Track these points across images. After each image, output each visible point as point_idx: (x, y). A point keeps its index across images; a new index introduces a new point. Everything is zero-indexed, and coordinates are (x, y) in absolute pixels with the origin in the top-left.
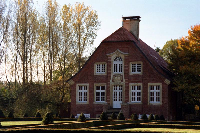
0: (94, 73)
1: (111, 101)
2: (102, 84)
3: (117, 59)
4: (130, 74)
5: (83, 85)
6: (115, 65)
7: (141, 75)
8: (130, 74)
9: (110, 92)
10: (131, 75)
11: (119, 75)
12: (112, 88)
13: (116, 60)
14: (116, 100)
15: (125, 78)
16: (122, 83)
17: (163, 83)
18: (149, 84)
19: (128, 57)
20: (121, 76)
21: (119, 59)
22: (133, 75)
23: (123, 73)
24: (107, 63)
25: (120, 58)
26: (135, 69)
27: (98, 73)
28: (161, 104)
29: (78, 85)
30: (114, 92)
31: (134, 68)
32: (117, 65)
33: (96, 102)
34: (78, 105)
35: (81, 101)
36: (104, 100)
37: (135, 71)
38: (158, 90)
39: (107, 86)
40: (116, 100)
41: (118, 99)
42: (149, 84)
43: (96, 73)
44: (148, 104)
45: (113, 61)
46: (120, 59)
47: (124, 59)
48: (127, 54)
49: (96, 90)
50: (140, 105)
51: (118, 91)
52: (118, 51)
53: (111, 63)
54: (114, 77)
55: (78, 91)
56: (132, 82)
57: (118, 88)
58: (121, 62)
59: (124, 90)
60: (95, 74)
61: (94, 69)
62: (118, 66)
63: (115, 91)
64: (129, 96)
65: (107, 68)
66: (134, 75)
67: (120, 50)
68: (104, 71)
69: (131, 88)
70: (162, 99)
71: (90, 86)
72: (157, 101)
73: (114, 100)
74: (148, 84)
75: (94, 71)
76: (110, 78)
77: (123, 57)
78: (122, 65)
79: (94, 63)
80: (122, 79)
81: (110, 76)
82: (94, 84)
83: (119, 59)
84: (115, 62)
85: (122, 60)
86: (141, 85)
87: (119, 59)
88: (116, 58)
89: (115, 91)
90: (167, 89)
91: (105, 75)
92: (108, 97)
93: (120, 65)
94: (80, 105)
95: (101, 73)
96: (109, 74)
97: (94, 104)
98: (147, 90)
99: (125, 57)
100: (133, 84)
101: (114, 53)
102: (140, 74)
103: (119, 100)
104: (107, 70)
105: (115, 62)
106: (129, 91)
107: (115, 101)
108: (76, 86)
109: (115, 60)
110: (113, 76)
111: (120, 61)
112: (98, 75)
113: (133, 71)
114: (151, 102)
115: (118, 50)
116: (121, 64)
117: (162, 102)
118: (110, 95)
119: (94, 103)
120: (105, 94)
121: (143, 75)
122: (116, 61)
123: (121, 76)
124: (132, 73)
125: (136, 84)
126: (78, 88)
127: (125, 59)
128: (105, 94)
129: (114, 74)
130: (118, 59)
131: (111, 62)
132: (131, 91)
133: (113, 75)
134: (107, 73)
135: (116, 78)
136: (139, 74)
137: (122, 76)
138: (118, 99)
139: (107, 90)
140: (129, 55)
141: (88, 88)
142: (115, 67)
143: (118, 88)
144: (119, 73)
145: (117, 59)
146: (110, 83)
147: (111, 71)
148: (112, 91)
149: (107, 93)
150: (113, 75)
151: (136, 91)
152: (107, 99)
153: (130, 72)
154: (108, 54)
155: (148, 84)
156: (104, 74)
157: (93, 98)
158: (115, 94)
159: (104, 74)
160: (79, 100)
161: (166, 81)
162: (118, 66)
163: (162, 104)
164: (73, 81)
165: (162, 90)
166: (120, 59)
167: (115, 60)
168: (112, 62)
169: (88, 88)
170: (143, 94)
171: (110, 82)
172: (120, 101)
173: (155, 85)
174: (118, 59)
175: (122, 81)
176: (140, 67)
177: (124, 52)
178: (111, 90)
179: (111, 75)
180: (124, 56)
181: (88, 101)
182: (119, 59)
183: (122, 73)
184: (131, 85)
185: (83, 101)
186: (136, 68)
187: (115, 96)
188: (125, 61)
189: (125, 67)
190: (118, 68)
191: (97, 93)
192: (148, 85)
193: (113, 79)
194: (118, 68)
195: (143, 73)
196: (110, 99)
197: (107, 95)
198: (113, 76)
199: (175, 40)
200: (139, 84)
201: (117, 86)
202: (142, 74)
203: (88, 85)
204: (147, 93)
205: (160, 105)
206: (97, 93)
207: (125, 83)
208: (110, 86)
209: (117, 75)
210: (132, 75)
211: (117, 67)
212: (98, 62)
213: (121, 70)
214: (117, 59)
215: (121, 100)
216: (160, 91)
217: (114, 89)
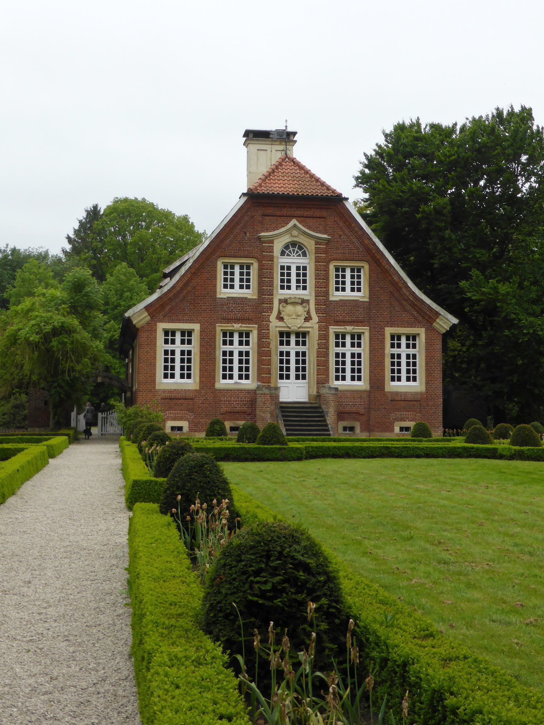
0: (215, 292)
1: (273, 380)
2: (243, 325)
3: (290, 252)
4: (331, 298)
5: (178, 330)
6: (282, 268)
7: (363, 302)
8: (331, 298)
9: (269, 354)
10: (334, 301)
11: (300, 301)
12: (274, 338)
13: (287, 252)
14: (288, 377)
15: (317, 311)
16: (307, 324)
17: (430, 330)
18: (389, 331)
19: (325, 246)
20: (304, 302)
21: (296, 249)
22: (341, 300)
23: (310, 293)
24: (260, 262)
25: (300, 248)
26: (344, 283)
27: (228, 290)
28: (423, 389)
29: (161, 326)
30: (281, 354)
31: (340, 280)
32: (289, 268)
33: (222, 383)
34: (164, 391)
35: (169, 380)
36: (247, 377)
37: (344, 290)
38: (413, 348)
39: (259, 334)
40: (288, 377)
41: (293, 373)
42: (389, 331)
43: (223, 293)
44: (387, 390)
45: (278, 258)
46: (300, 252)
47: (314, 251)
48: (325, 236)
49: (222, 346)
50: (364, 391)
51: (293, 348)
52: (295, 226)
53: (273, 261)
54: (285, 305)
55: (161, 346)
56: (337, 323)
57: (293, 339)
58: (302, 261)
59: (316, 347)
60: (218, 296)
61: (215, 278)
62: (293, 272)
63: (285, 348)
64: (328, 368)
65: (260, 276)
66: (343, 303)
67: (300, 222)
68: (248, 287)
69: (332, 340)
70: (427, 377)
71: (202, 331)
72: (408, 379)
73: (281, 377)
74: (386, 328)
75: (215, 286)
76: (271, 309)
77: (310, 245)
78: (305, 268)
79: (216, 260)
80: (308, 312)
81: (271, 302)
82: (215, 328)
83: (297, 252)
84: (284, 261)
85: (304, 254)
86: (363, 333)
87: (297, 252)
88: (287, 247)
89: (285, 348)
90: (439, 346)
91: (252, 299)
92: (263, 366)
93: (298, 268)
94: (170, 391)
95: (237, 292)
96: (267, 297)
97: (217, 390)
98: (383, 349)
99: (316, 245)
100: (340, 329)
101: (283, 229)
102: (361, 300)
103: (297, 377)
104: (260, 284)
105: (284, 261)
106: (327, 348)
107: (285, 381)
108: (155, 331)
109: (283, 253)
110: (281, 301)
111: (299, 256)
112: (228, 298)
113: (337, 289)
114: (393, 383)
115: (294, 222)
116: (301, 265)
117: (427, 383)
118: (269, 363)
119: (217, 386)
120: (253, 358)
121: (370, 303)
122: (288, 255)
123: (304, 305)
124: (336, 296)
125: (349, 328)
126: (160, 337)
127: (317, 251)
128: (253, 358)
129: (282, 297)
130: (294, 251)
131: (271, 259)
132: (333, 350)
133: (280, 300)
134: (261, 292)
135: (289, 308)
136: (358, 300)
137: (308, 301)
138: (293, 373)
139: (260, 344)
140: (328, 241)
141: (195, 338)
142: (282, 274)
143: (293, 339)
144: (294, 294)
145: (290, 252)
146: (271, 324)
147: (272, 285)
148: (277, 348)
149: (260, 354)
150: (280, 300)
151: (348, 350)
152: (259, 374)
153: (330, 292)
154: (263, 234)
155: (386, 328)
156: (250, 294)
157: (214, 370)
158: (285, 358)
159: (249, 297)
160: (166, 376)
161: (441, 323)
162: (293, 272)
163: (427, 389)
164: (147, 314)
165: (427, 349)
166: (300, 252)
167: (283, 253)
168: (275, 260)
169: (195, 338)
170: (371, 359)
171: (271, 320)
172: (301, 381)
173: (404, 334)
174: (294, 251)
175: (308, 319)
176: (359, 277)
177: (309, 228)
178: (273, 346)
179: (274, 300)
180: (313, 243)
181: (198, 380)
182: (296, 249)
183: (308, 294)
184: (333, 329)
185: (177, 378)
186: (348, 280)
187: (285, 365)
188: (316, 257)
189: (317, 277)
190: (293, 278)
191: (224, 353)
192: (386, 332)
193: (279, 313)
194: (293, 278)
195: (370, 298)
196: (270, 374)
197: (260, 362)
198: (281, 301)
199: (144, 200)
200: (357, 329)
201: (288, 335)
202: (367, 300)
203: (196, 327)
204: (383, 355)
205: (421, 393)
206: (224, 353)
207: (317, 326)
208: (270, 334)
209: (293, 300)
210: (337, 301)
211: (289, 275)
212: (230, 256)
213: (245, 284)
214: (291, 249)
215: (304, 377)
216: (420, 352)
217: (282, 343)
